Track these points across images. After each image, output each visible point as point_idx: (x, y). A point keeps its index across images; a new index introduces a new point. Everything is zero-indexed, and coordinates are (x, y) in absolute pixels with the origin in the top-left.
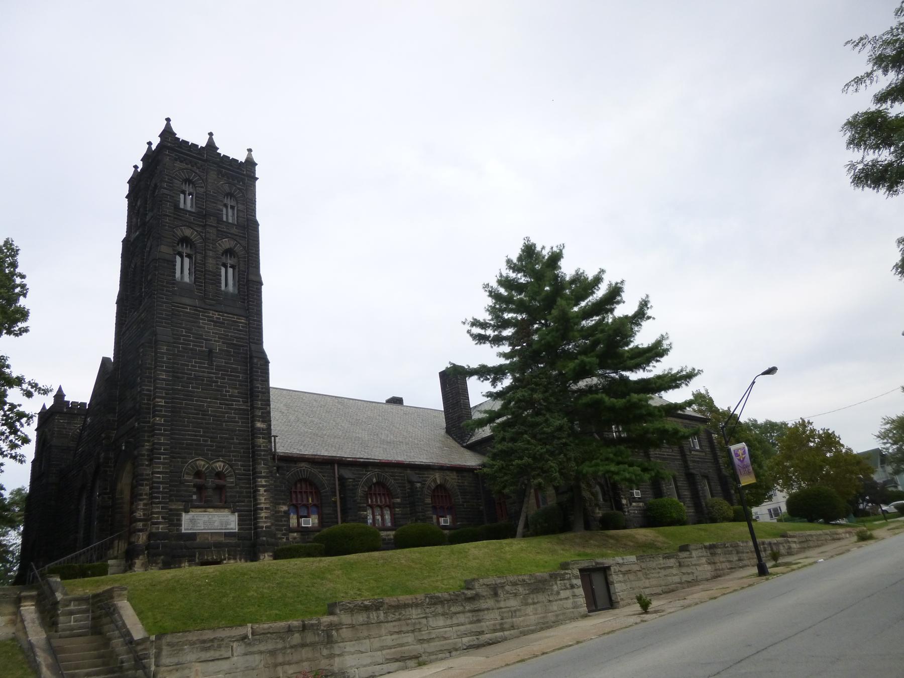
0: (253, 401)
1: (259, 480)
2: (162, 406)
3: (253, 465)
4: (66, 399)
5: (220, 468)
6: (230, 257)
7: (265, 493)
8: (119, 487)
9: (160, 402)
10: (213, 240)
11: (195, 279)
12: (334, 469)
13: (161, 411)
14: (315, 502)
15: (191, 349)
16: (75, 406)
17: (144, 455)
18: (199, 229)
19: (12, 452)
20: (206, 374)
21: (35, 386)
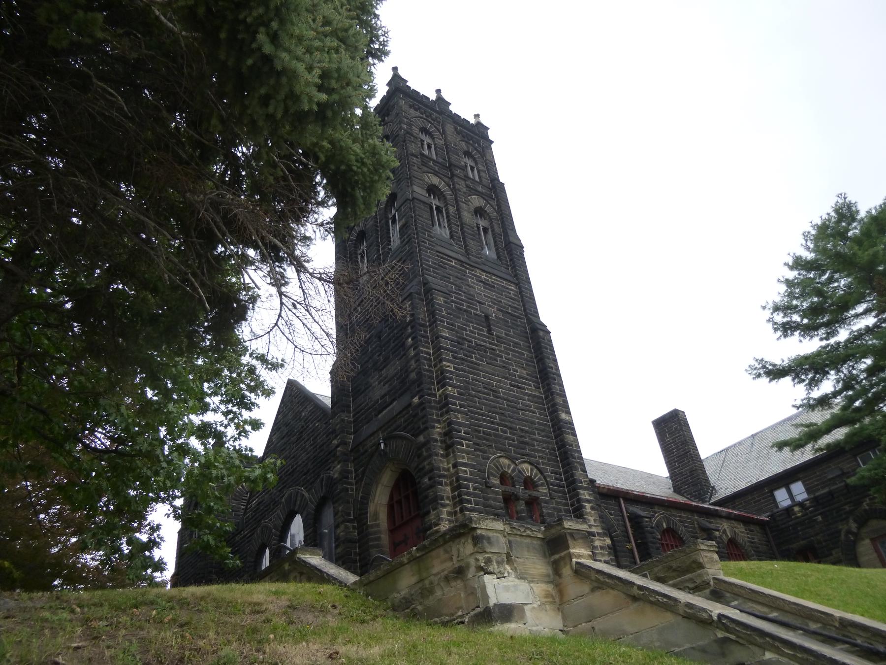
0: (548, 385)
1: (582, 491)
2: (452, 373)
3: (565, 472)
5: (528, 471)
6: (481, 217)
7: (593, 512)
8: (371, 508)
9: (449, 366)
10: (464, 192)
11: (450, 233)
12: (620, 506)
13: (451, 379)
15: (466, 311)
17: (436, 441)
18: (446, 180)
19: (235, 444)
20: (487, 345)
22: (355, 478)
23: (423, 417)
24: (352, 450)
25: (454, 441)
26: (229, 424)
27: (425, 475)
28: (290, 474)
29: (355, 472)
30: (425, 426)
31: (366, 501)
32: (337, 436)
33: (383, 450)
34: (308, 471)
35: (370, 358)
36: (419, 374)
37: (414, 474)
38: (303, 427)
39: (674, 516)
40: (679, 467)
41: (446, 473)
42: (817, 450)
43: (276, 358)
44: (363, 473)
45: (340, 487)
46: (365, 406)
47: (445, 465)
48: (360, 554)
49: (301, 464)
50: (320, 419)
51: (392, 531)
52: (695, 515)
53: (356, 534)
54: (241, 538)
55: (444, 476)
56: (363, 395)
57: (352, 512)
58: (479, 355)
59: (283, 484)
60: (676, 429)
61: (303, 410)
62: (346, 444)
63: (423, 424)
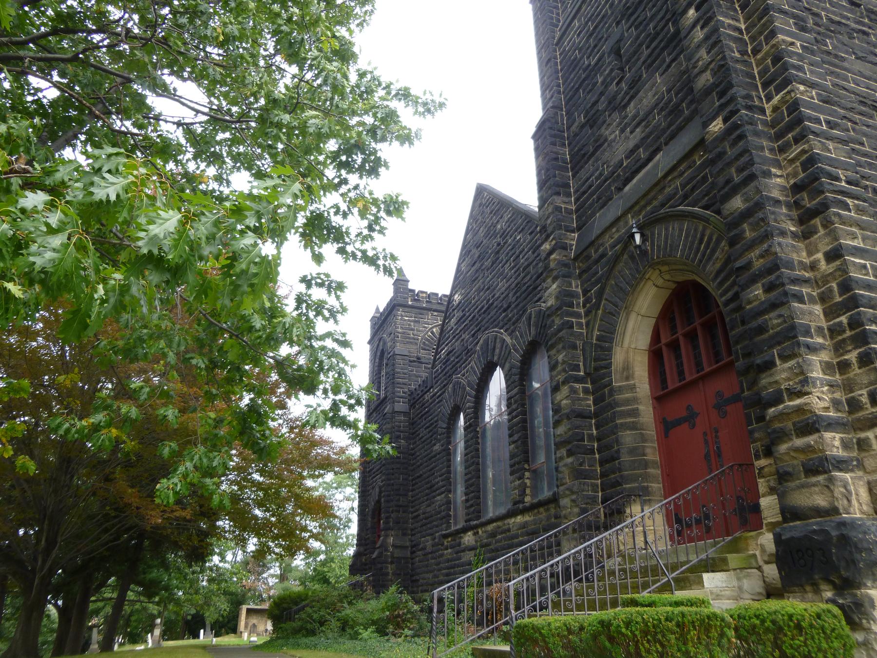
2: (801, 58)
4: (411, 286)
8: (618, 357)
9: (792, 44)
16: (423, 297)
17: (777, 202)
20: (853, 25)
21: (405, 95)
22: (584, 306)
23: (741, 155)
24: (576, 259)
25: (826, 198)
26: (349, 209)
27: (754, 280)
28: (484, 312)
29: (584, 295)
30: (745, 173)
31: (607, 345)
32: (548, 237)
33: (639, 246)
34: (509, 307)
35: (602, 94)
36: (722, 69)
37: (711, 287)
38: (499, 244)
41: (807, 275)
43: (430, 93)
44: (600, 294)
45: (558, 321)
46: (597, 179)
47: (804, 257)
48: (599, 440)
49: (499, 297)
50: (523, 229)
51: (660, 399)
53: (591, 402)
54: (432, 397)
55: (806, 281)
56: (593, 159)
57: (581, 364)
58: (839, 41)
59: (476, 326)
61: (498, 221)
62: (564, 247)
63: (740, 170)
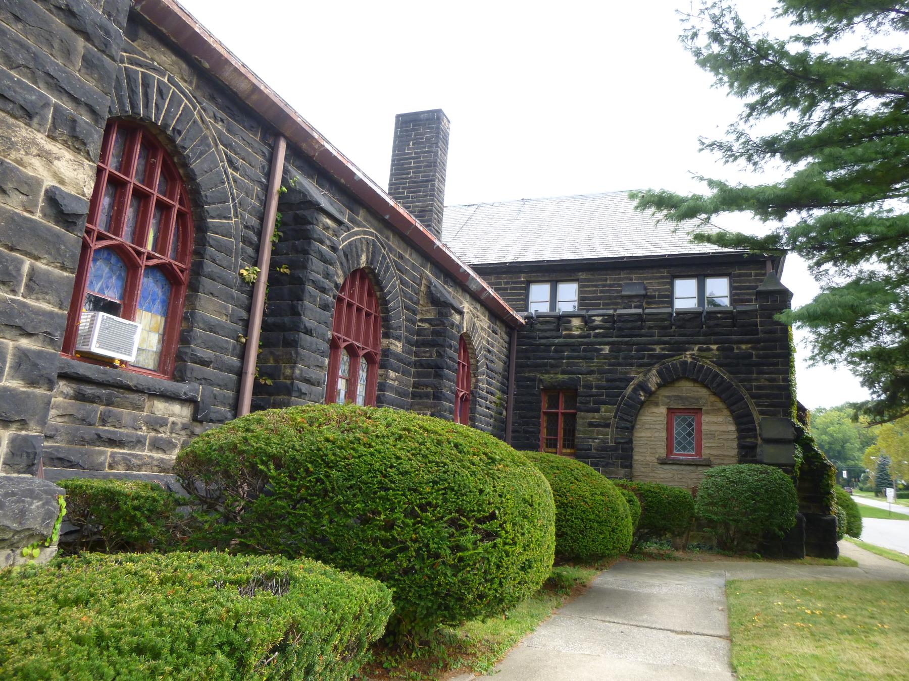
12: (271, 160)
14: (166, 259)
39: (391, 250)
40: (408, 197)
42: (700, 238)
52: (429, 265)
60: (428, 139)
